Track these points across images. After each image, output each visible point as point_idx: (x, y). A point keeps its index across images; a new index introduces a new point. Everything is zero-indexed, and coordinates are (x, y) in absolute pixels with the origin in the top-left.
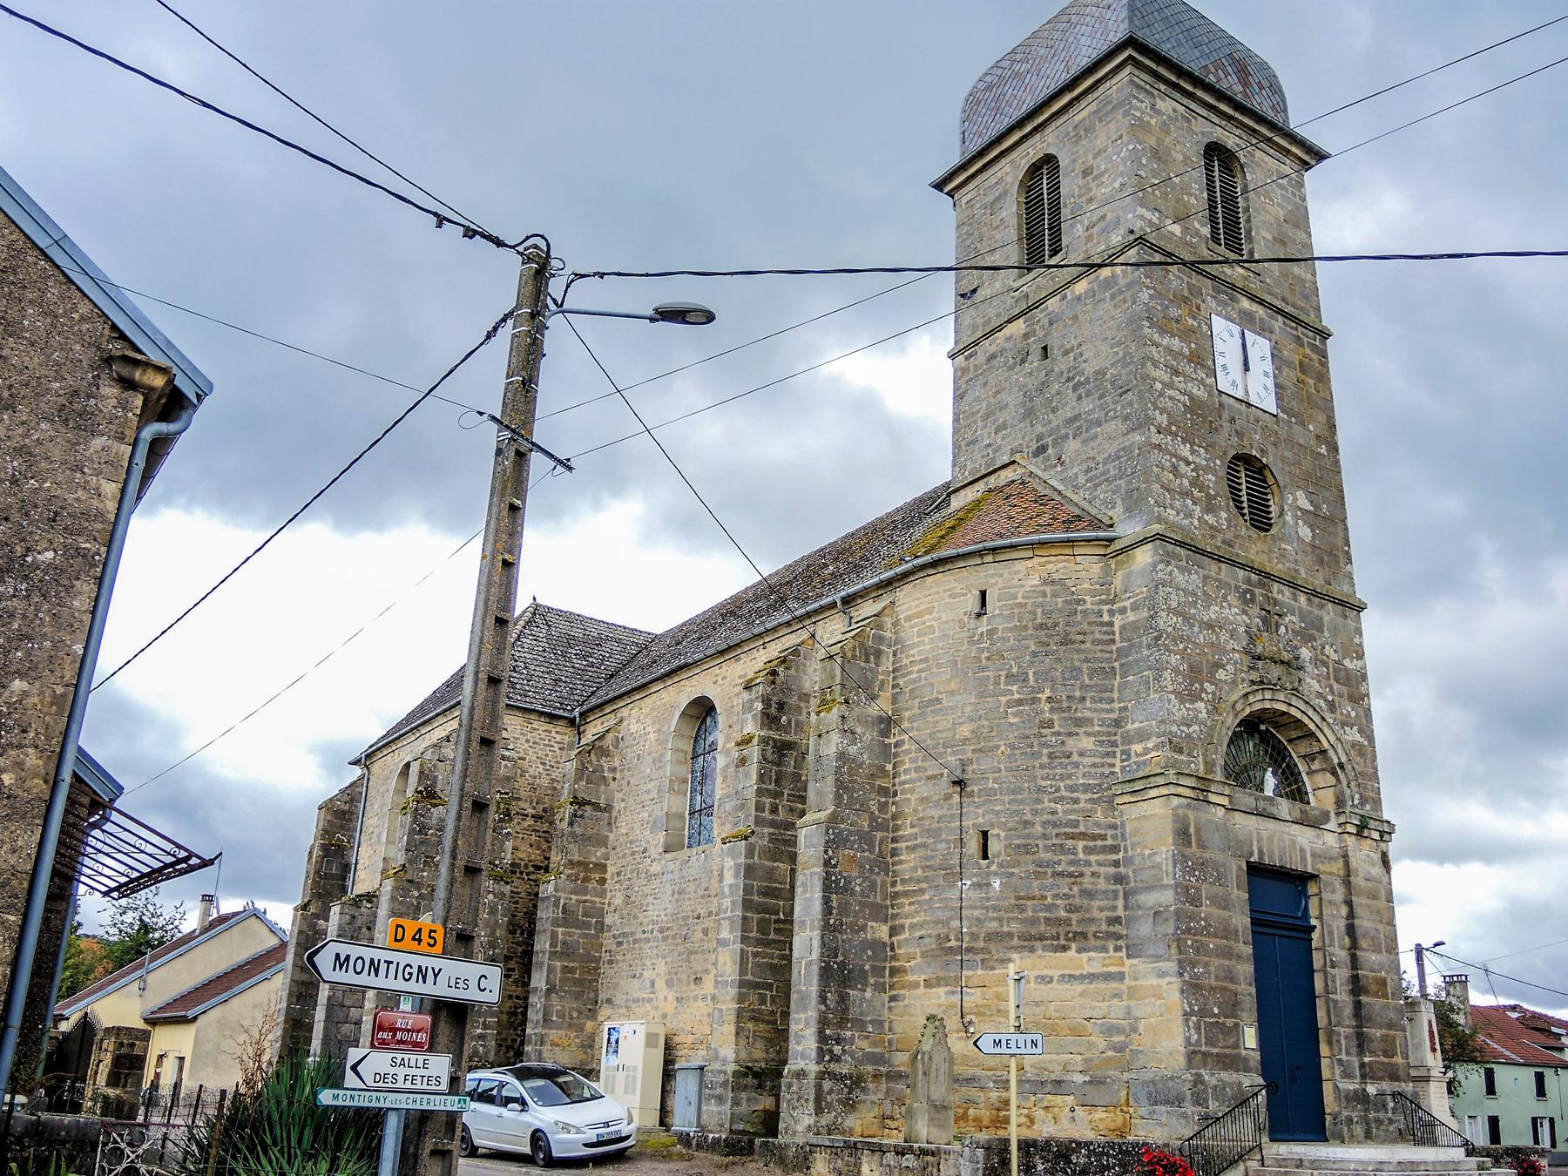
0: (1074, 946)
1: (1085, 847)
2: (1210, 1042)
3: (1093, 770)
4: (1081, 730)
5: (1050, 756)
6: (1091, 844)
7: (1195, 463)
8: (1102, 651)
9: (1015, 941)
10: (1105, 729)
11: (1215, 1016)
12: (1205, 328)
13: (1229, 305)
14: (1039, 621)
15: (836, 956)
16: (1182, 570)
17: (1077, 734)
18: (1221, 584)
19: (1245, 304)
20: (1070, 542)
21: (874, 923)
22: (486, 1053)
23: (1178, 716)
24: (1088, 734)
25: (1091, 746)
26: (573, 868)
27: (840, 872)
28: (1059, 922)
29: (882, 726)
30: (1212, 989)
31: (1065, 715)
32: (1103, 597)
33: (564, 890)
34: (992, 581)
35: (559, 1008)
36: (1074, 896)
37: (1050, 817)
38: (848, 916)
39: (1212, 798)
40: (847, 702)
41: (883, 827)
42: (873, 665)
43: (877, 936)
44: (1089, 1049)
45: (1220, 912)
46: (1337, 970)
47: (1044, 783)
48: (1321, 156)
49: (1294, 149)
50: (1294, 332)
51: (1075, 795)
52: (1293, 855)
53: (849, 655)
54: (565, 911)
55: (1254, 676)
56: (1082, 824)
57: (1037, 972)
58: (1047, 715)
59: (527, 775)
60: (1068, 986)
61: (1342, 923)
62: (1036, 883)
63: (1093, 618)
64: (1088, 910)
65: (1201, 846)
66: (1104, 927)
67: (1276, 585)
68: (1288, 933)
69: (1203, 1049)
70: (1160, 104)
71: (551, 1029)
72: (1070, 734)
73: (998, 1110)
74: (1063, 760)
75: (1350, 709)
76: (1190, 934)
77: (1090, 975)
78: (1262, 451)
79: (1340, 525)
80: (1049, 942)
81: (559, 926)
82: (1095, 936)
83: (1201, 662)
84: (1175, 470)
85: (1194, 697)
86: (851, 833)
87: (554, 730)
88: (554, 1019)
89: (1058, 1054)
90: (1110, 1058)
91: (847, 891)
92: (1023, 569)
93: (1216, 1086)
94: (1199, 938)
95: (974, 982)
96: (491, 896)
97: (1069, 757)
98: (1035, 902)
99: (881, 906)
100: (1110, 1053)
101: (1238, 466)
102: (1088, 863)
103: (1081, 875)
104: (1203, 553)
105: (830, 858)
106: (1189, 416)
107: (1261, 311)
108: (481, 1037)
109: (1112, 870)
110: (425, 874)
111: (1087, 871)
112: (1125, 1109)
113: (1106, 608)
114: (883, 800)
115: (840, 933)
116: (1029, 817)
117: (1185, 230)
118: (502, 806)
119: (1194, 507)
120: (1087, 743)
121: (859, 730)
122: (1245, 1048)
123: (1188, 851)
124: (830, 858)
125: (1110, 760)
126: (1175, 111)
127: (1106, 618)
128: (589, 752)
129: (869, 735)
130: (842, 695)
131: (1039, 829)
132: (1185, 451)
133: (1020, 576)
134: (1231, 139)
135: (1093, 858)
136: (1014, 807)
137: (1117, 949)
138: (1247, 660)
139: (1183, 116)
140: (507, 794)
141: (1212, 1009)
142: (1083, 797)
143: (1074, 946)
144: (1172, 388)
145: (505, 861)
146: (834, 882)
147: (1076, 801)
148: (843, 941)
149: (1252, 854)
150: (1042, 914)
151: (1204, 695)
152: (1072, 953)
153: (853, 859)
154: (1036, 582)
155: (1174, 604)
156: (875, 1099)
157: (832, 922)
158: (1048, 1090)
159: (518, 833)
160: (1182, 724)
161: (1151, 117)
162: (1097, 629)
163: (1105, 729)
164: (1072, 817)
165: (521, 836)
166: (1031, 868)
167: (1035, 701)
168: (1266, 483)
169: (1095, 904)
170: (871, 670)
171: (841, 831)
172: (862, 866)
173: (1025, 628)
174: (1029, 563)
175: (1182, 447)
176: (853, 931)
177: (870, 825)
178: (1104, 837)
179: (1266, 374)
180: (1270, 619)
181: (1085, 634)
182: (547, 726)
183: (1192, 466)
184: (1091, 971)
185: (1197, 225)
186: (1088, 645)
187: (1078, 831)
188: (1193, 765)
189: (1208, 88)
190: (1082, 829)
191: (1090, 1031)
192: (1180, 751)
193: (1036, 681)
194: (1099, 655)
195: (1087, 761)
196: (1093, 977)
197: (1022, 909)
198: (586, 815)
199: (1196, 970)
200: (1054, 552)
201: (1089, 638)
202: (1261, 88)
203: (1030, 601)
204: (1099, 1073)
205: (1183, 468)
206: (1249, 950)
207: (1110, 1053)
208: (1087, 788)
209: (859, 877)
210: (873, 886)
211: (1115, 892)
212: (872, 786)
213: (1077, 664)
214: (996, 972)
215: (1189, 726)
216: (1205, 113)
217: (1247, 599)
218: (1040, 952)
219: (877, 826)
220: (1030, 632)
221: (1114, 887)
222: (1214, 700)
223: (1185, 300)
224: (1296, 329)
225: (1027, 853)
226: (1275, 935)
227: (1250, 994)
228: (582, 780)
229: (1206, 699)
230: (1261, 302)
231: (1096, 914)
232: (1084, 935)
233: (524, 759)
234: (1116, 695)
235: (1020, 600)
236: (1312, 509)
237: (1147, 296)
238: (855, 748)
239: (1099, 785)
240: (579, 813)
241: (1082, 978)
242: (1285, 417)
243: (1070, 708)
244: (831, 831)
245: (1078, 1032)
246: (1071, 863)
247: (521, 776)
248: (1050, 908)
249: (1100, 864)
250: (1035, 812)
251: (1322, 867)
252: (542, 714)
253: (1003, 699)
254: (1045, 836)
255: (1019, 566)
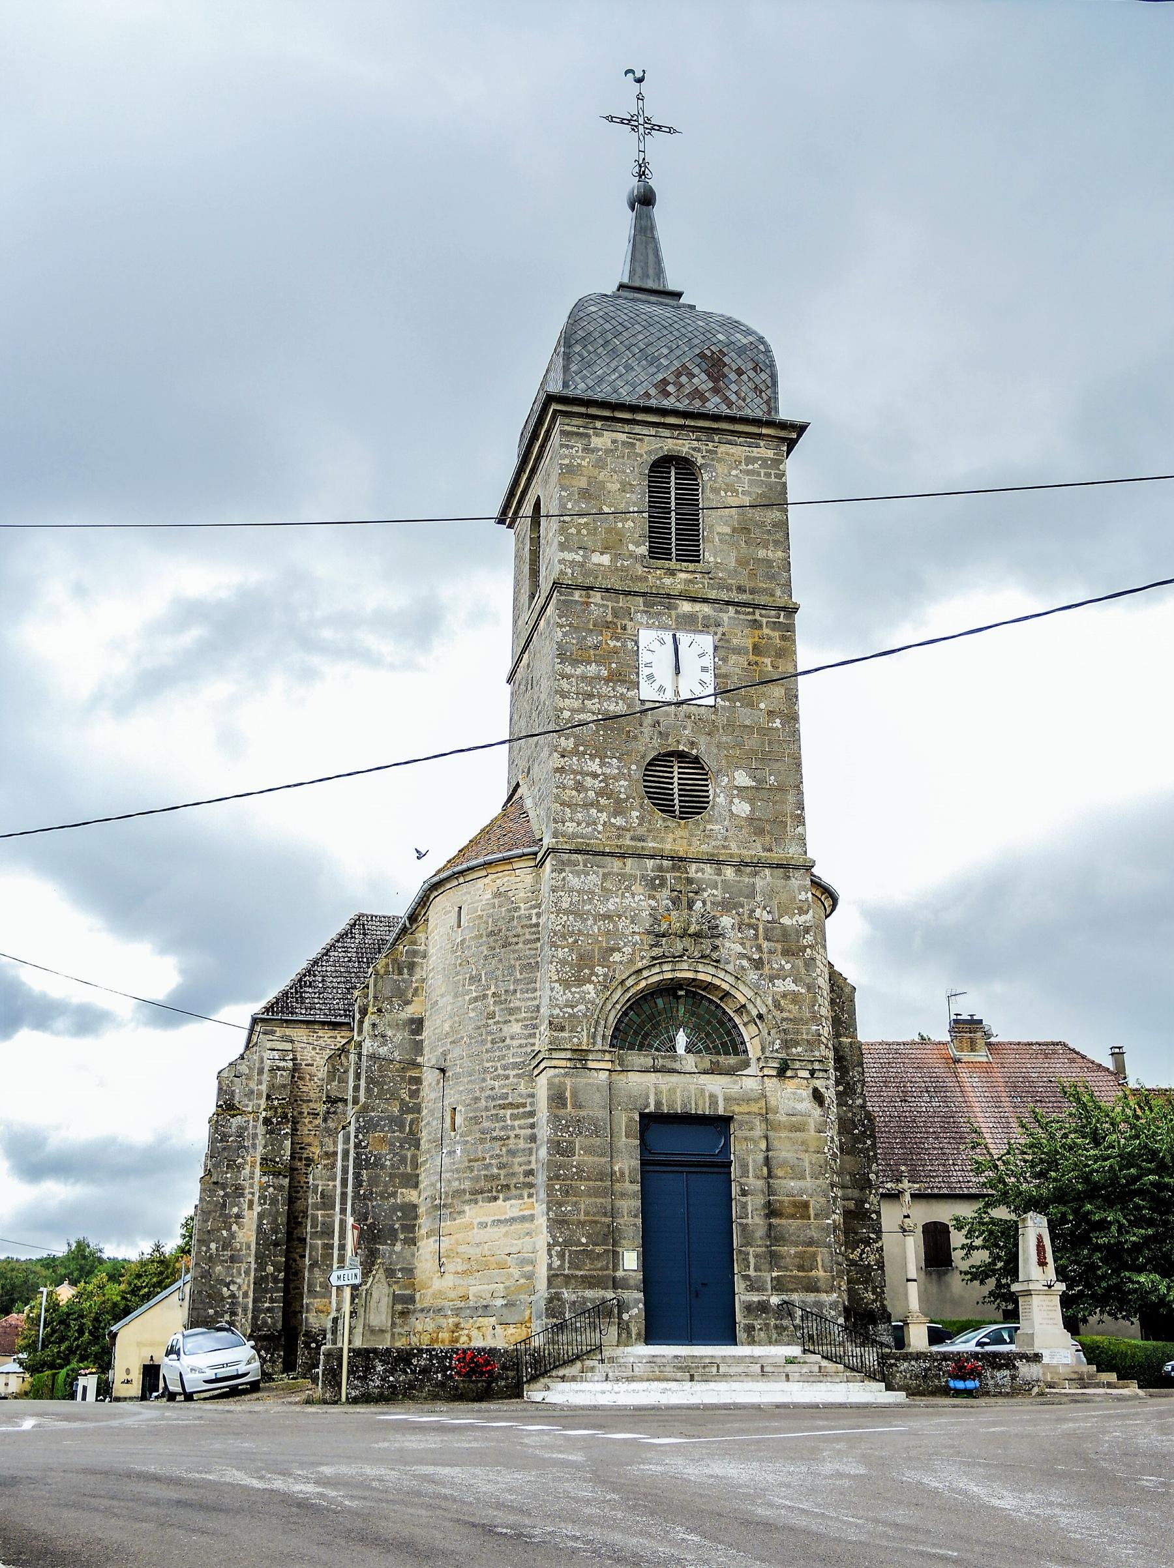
0: (501, 1196)
1: (512, 1115)
2: (574, 1265)
3: (519, 1050)
4: (512, 1018)
5: (493, 1042)
6: (516, 1111)
7: (603, 774)
8: (530, 949)
9: (468, 1197)
10: (529, 1015)
11: (583, 1244)
12: (630, 644)
13: (665, 614)
14: (490, 929)
15: (366, 1219)
16: (577, 874)
17: (510, 1021)
18: (623, 877)
19: (686, 607)
20: (507, 860)
21: (404, 1190)
22: (274, 1324)
23: (561, 1000)
24: (517, 1021)
25: (519, 1031)
26: (329, 1159)
27: (370, 1152)
28: (495, 1177)
29: (414, 1027)
30: (581, 1224)
31: (503, 1006)
32: (534, 902)
33: (321, 1178)
34: (465, 898)
35: (322, 1280)
36: (502, 1156)
37: (490, 1092)
38: (377, 1186)
39: (591, 1065)
40: (380, 1010)
41: (410, 1111)
42: (406, 976)
43: (407, 1200)
44: (508, 1279)
45: (596, 1159)
46: (749, 1198)
47: (488, 1065)
48: (801, 429)
49: (765, 431)
50: (750, 617)
51: (507, 1072)
52: (700, 1102)
53: (382, 971)
54: (323, 1196)
55: (656, 952)
56: (510, 1095)
57: (479, 1220)
58: (492, 1008)
59: (315, 1078)
60: (496, 1229)
61: (760, 1157)
62: (480, 1147)
63: (525, 922)
64: (511, 1166)
65: (578, 1106)
66: (522, 1179)
67: (694, 866)
68: (693, 1169)
69: (566, 1272)
70: (596, 442)
71: (315, 1298)
72: (506, 1022)
73: (453, 1332)
74: (500, 1044)
75: (783, 962)
76: (558, 1180)
77: (513, 1218)
78: (692, 743)
79: (792, 792)
80: (486, 1195)
81: (318, 1210)
82: (515, 1187)
83: (593, 950)
84: (579, 787)
85: (581, 982)
86: (381, 1119)
87: (338, 1036)
88: (318, 1289)
89: (488, 1284)
90: (522, 1285)
91: (377, 1166)
92: (482, 886)
93: (574, 1302)
94: (569, 1182)
95: (446, 1231)
96: (271, 1190)
97: (504, 1041)
98: (479, 1163)
99: (411, 1175)
100: (522, 1281)
101: (672, 761)
102: (513, 1128)
103: (508, 1138)
104: (604, 854)
105: (361, 1141)
106: (601, 733)
107: (706, 609)
108: (269, 1310)
109: (529, 1131)
110: (229, 1175)
111: (512, 1134)
112: (528, 1325)
113: (535, 911)
114: (414, 1087)
115: (369, 1200)
116: (478, 1094)
117: (616, 557)
118: (279, 1110)
119: (599, 814)
120: (516, 1028)
121: (389, 1033)
122: (624, 1270)
123: (562, 1112)
124: (361, 1141)
125: (531, 1041)
126: (614, 442)
127: (534, 921)
128: (340, 1056)
129: (400, 1036)
130: (374, 1006)
131: (483, 1103)
132: (594, 766)
133: (480, 892)
134: (683, 446)
135: (516, 1123)
136: (470, 1087)
137: (530, 1196)
138: (651, 940)
139: (623, 443)
140: (284, 1099)
141: (579, 1240)
142: (512, 1073)
143: (501, 1196)
144: (583, 712)
145: (285, 1158)
146: (364, 1160)
147: (507, 1077)
148: (373, 1207)
149: (647, 1106)
150: (483, 1173)
151: (594, 978)
152: (500, 1202)
153: (383, 1140)
154: (489, 896)
155: (565, 905)
156: (403, 1332)
157: (362, 1192)
158: (479, 1314)
159: (309, 1130)
160: (566, 1006)
161: (583, 459)
162: (527, 930)
163: (529, 1015)
164: (504, 1091)
165: (313, 1133)
166: (478, 1135)
167: (485, 996)
168: (704, 769)
169: (517, 1160)
170: (404, 981)
171: (372, 1118)
172: (392, 1144)
173: (481, 936)
174: (486, 880)
175: (589, 763)
176: (382, 1198)
177: (401, 1110)
178: (524, 1105)
179: (704, 669)
180: (683, 900)
181: (519, 936)
182: (331, 1033)
183: (601, 778)
184: (512, 1215)
185: (631, 547)
186: (520, 945)
187: (507, 1102)
188: (575, 1040)
189: (647, 410)
190: (510, 1100)
191: (509, 1264)
192: (562, 1029)
193: (486, 981)
194: (528, 952)
195: (515, 1043)
196: (513, 1220)
197: (471, 1168)
198: (339, 1111)
199: (563, 1209)
200: (500, 869)
201: (522, 939)
202: (740, 372)
203: (485, 912)
204: (514, 1297)
205: (589, 782)
206: (637, 1187)
207: (522, 1281)
208: (515, 1066)
209: (389, 1154)
210: (403, 1160)
211: (531, 1149)
212: (403, 1078)
213: (512, 962)
214: (457, 1222)
215: (572, 1007)
216: (652, 431)
217: (654, 884)
218: (480, 1203)
219: (405, 1109)
220: (484, 939)
221: (530, 1146)
222: (605, 980)
223: (607, 625)
224: (754, 613)
225: (476, 1124)
226: (682, 1172)
227: (635, 1225)
228: (333, 1081)
229: (596, 981)
230: (705, 600)
231: (517, 1169)
232: (507, 1186)
233: (312, 1065)
234: (538, 985)
235: (479, 913)
236: (754, 784)
237: (560, 634)
238: (386, 1048)
239: (523, 1062)
240: (332, 1110)
241: (506, 1221)
242: (727, 703)
243: (506, 1000)
244: (361, 1119)
245: (502, 1266)
246: (503, 1128)
247: (310, 1080)
248: (487, 1167)
249: (521, 1128)
250: (482, 1089)
251: (736, 1109)
252: (323, 1023)
253: (467, 998)
254: (487, 1109)
255: (480, 883)
